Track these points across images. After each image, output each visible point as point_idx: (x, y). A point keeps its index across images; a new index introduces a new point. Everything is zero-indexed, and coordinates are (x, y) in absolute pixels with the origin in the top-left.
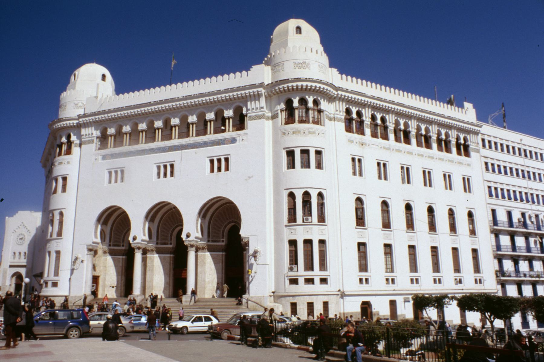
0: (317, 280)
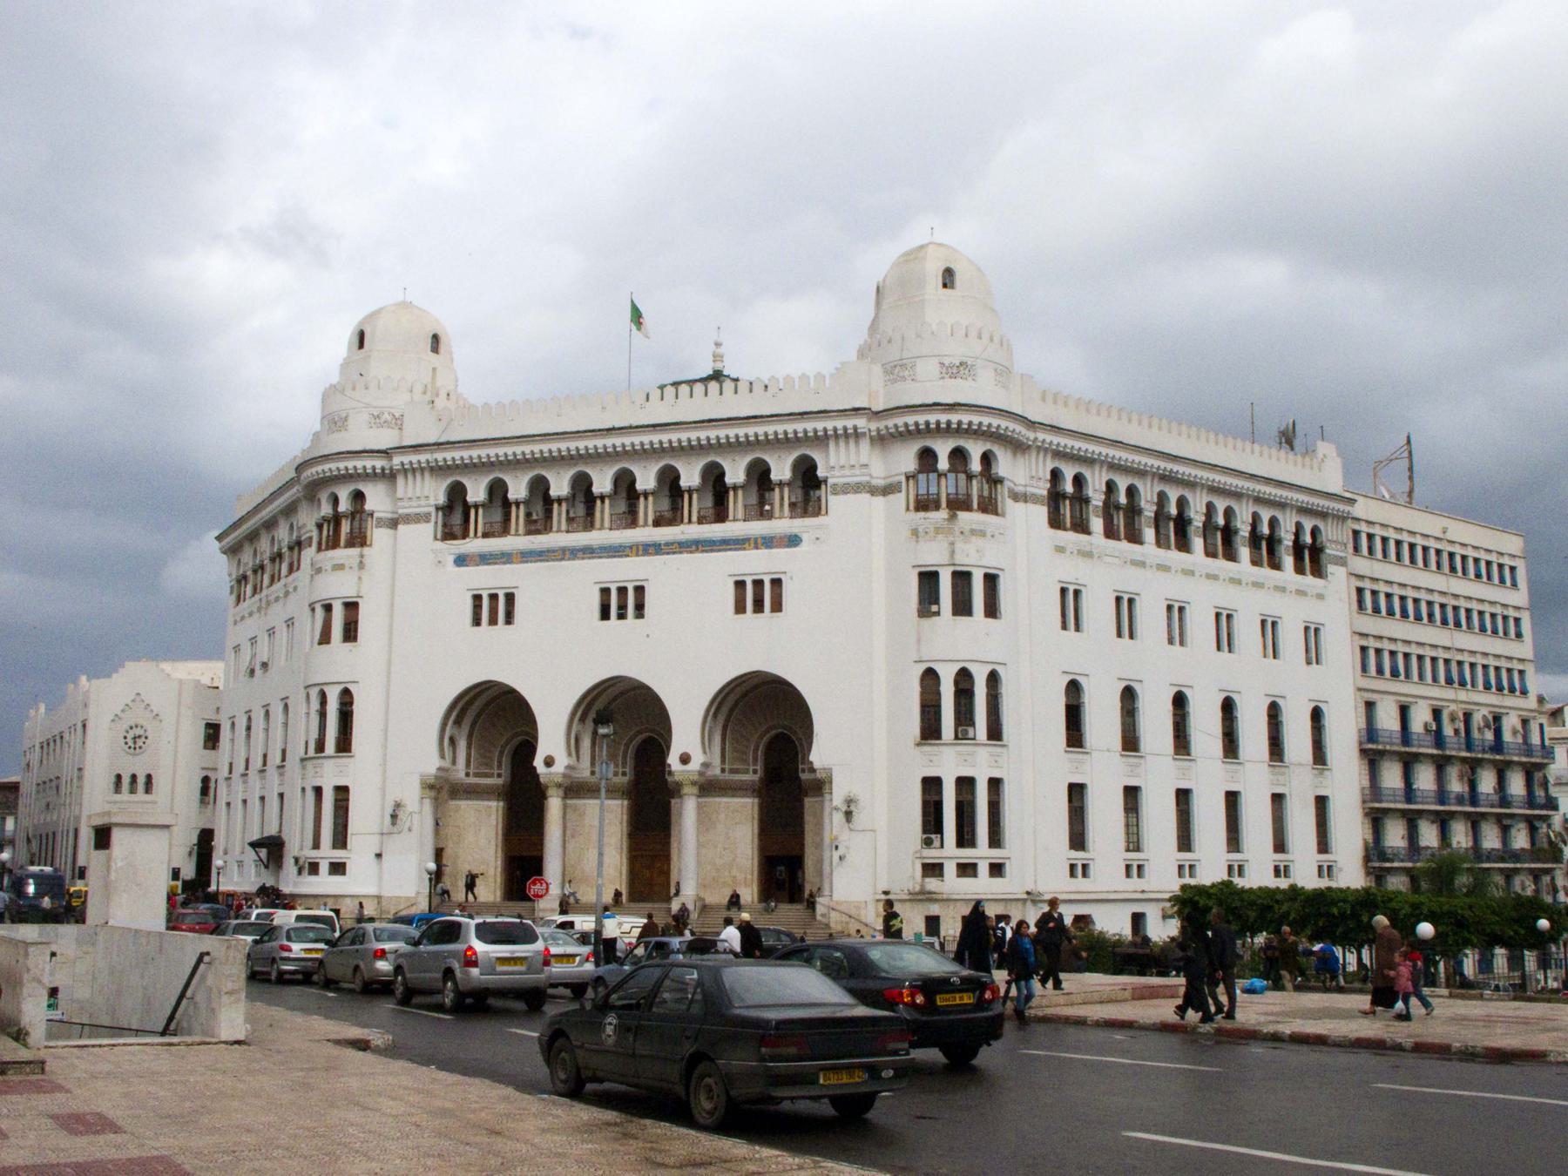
0: (983, 869)
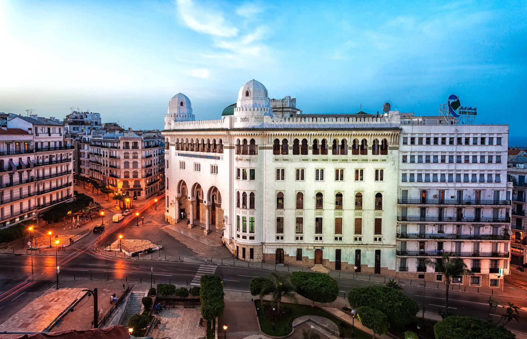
0: (248, 238)
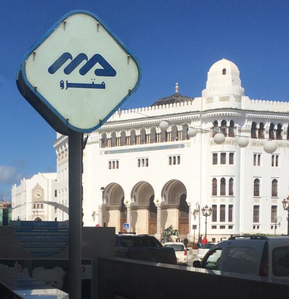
0: (227, 227)
